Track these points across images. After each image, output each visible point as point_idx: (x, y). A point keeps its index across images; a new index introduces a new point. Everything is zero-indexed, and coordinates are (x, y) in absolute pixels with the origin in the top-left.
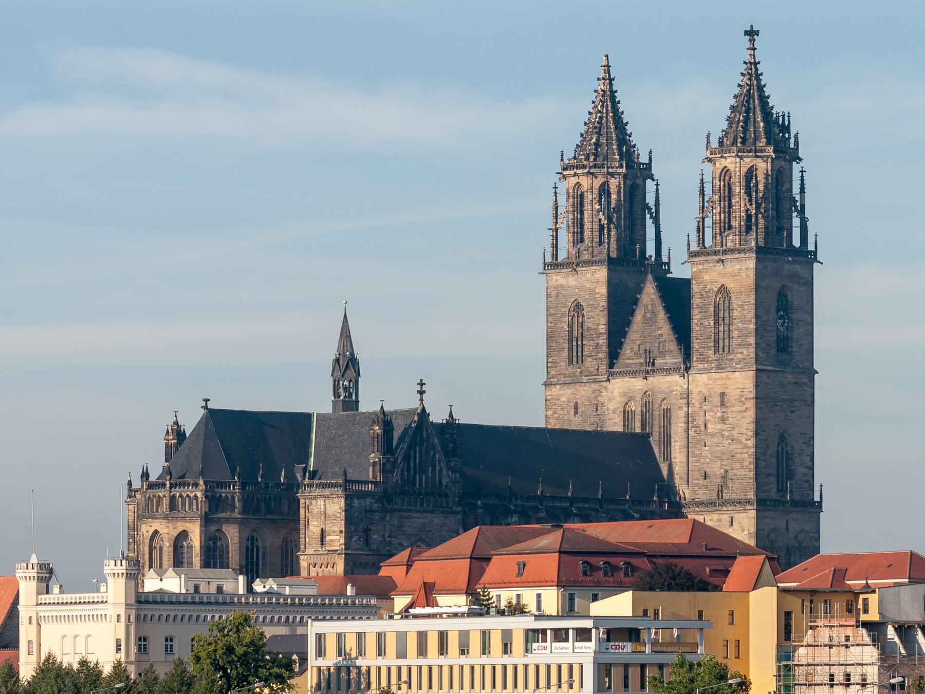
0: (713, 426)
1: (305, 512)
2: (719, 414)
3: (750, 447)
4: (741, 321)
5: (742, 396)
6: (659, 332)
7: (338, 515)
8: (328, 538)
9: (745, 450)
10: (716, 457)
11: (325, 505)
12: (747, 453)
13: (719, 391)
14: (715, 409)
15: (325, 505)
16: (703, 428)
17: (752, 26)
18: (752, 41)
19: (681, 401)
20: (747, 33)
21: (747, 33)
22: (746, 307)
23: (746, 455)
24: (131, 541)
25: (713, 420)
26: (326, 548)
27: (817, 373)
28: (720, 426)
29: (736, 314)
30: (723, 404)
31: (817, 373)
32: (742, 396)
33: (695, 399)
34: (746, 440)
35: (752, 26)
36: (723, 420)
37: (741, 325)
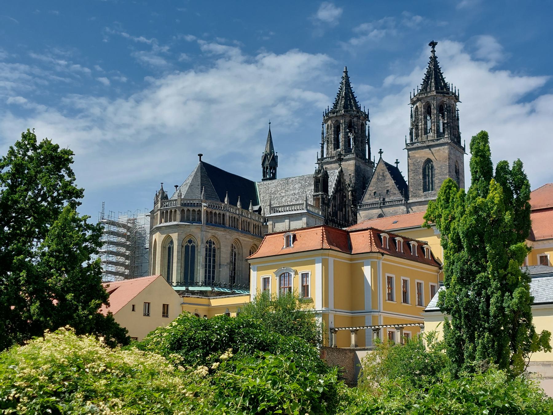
4: (440, 175)
6: (387, 185)
37: (440, 177)
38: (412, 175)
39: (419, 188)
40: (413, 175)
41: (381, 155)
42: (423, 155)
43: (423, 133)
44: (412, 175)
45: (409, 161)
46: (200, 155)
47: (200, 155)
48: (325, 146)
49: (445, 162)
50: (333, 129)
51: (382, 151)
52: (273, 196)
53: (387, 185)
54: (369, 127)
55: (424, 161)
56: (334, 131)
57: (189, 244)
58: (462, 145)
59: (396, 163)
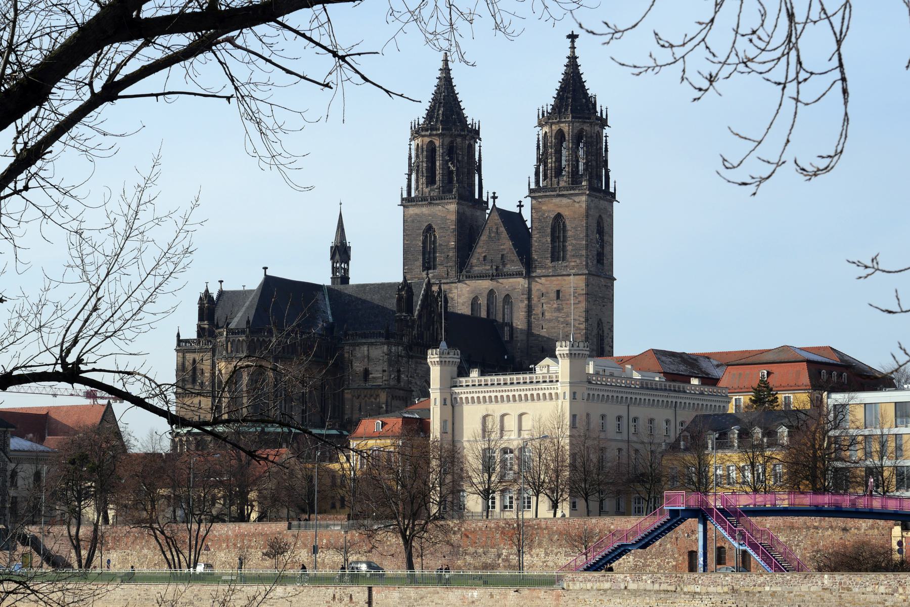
2: (555, 306)
3: (583, 329)
5: (576, 292)
6: (502, 247)
7: (381, 358)
8: (371, 376)
9: (578, 332)
11: (368, 350)
12: (580, 333)
13: (555, 289)
14: (552, 302)
15: (368, 350)
16: (541, 316)
17: (573, 32)
18: (573, 42)
19: (522, 296)
20: (569, 37)
21: (569, 37)
22: (579, 228)
23: (579, 335)
27: (616, 280)
28: (556, 314)
29: (569, 233)
30: (558, 297)
31: (616, 280)
32: (576, 292)
34: (579, 324)
35: (573, 32)
36: (559, 310)
37: (574, 242)
40: (538, 236)
42: (553, 206)
43: (553, 175)
45: (534, 215)
46: (265, 268)
47: (265, 268)
48: (414, 177)
49: (582, 221)
50: (425, 153)
53: (502, 247)
54: (480, 146)
55: (553, 216)
56: (427, 157)
59: (518, 206)
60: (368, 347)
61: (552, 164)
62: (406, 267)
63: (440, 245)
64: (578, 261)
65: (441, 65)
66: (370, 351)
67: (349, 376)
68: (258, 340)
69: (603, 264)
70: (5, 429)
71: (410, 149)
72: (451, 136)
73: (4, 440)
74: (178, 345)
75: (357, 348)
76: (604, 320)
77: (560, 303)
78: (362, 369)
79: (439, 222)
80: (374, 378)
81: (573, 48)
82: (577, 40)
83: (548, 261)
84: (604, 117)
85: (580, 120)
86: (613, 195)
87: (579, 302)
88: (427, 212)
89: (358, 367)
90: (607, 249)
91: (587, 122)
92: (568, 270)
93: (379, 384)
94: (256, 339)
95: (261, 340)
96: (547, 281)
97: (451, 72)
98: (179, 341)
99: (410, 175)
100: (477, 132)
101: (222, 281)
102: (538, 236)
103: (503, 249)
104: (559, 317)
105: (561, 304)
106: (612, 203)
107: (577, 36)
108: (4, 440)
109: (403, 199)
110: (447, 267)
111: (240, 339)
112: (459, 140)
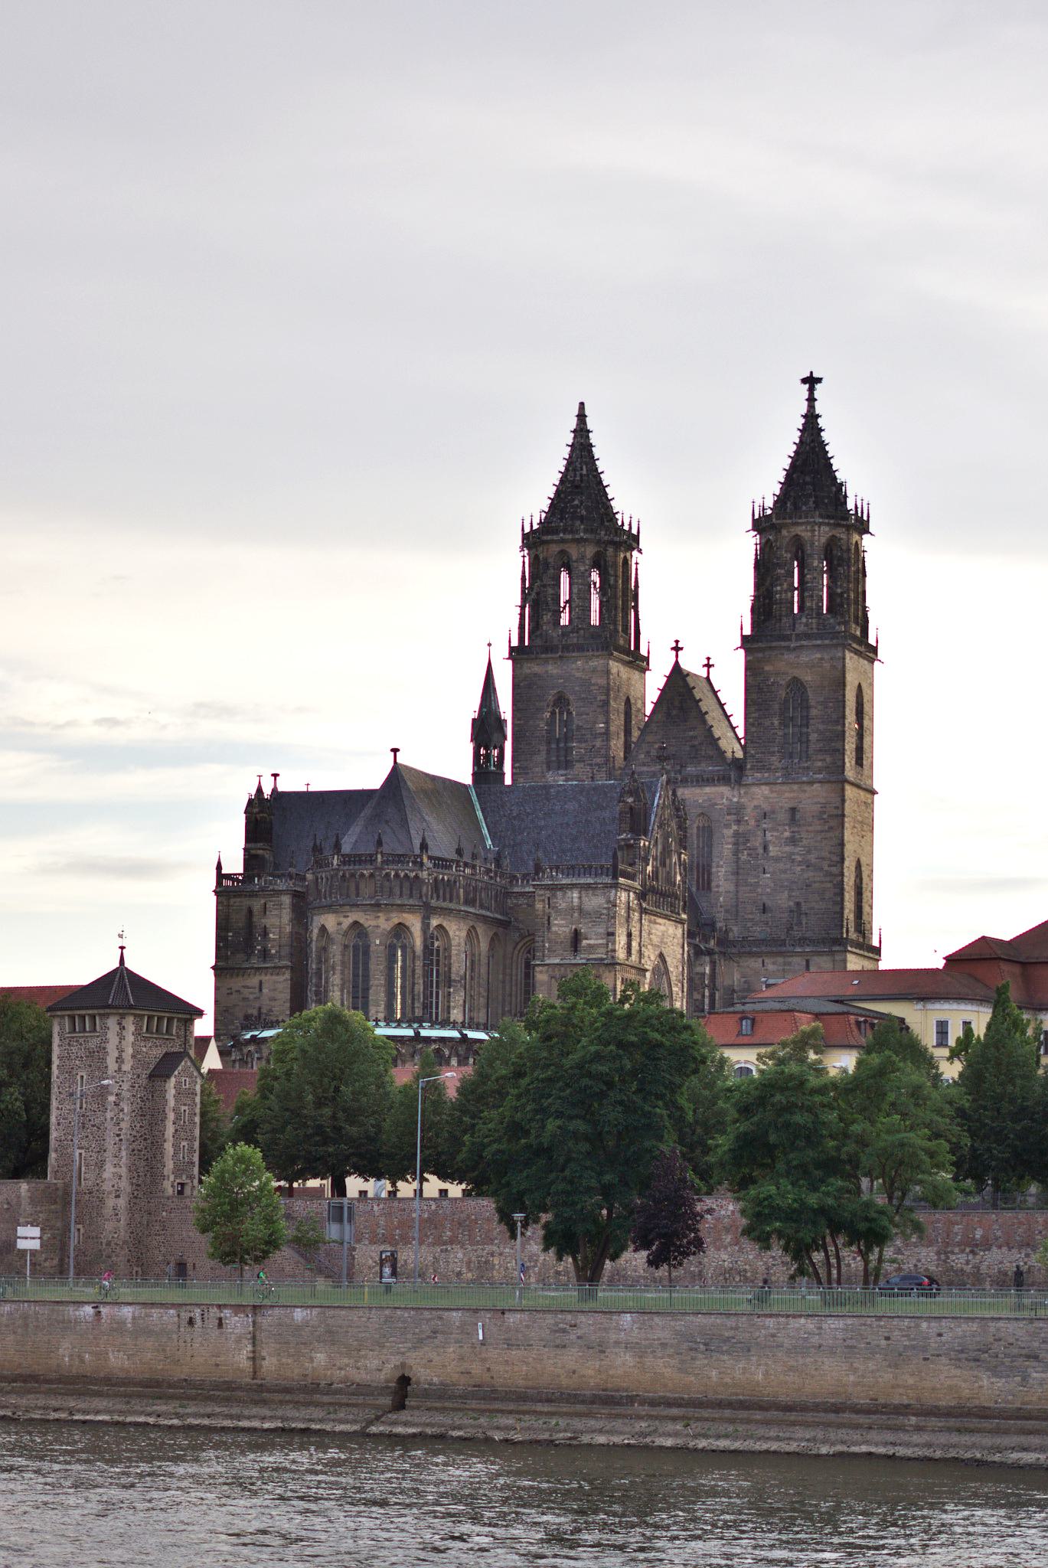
0: (778, 848)
1: (544, 907)
2: (787, 834)
5: (825, 812)
6: (691, 733)
7: (605, 911)
8: (585, 942)
10: (781, 887)
12: (830, 882)
13: (787, 806)
15: (580, 898)
16: (761, 851)
17: (811, 373)
18: (811, 390)
19: (728, 817)
20: (804, 381)
21: (804, 381)
22: (831, 704)
24: (221, 944)
25: (777, 842)
26: (582, 956)
28: (787, 849)
29: (814, 712)
33: (750, 816)
34: (830, 866)
35: (811, 373)
36: (793, 841)
38: (753, 715)
39: (772, 750)
40: (756, 715)
41: (677, 656)
44: (753, 715)
46: (395, 751)
47: (395, 751)
51: (680, 645)
52: (516, 822)
53: (691, 733)
57: (395, 941)
58: (872, 641)
59: (704, 666)
60: (580, 893)
61: (781, 594)
62: (517, 765)
63: (579, 728)
64: (828, 759)
65: (573, 423)
66: (583, 899)
67: (543, 941)
68: (397, 875)
69: (861, 765)
70: (188, 1017)
71: (524, 562)
72: (598, 542)
73: (186, 1036)
74: (219, 883)
75: (559, 894)
76: (863, 860)
77: (796, 829)
78: (567, 930)
79: (577, 688)
80: (589, 945)
81: (811, 400)
82: (818, 386)
83: (774, 758)
84: (865, 518)
85: (832, 521)
86: (875, 650)
87: (831, 828)
88: (555, 671)
89: (561, 927)
90: (866, 740)
91: (843, 526)
92: (811, 774)
93: (599, 956)
94: (393, 873)
95: (402, 875)
96: (772, 792)
97: (590, 434)
98: (220, 876)
99: (522, 608)
100: (636, 539)
101: (278, 775)
102: (756, 715)
103: (692, 737)
104: (794, 854)
105: (798, 832)
106: (873, 663)
107: (819, 380)
108: (186, 1036)
109: (512, 649)
110: (591, 765)
111: (365, 872)
112: (610, 550)
